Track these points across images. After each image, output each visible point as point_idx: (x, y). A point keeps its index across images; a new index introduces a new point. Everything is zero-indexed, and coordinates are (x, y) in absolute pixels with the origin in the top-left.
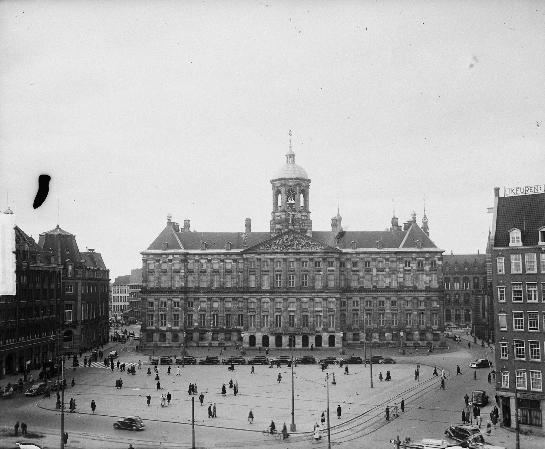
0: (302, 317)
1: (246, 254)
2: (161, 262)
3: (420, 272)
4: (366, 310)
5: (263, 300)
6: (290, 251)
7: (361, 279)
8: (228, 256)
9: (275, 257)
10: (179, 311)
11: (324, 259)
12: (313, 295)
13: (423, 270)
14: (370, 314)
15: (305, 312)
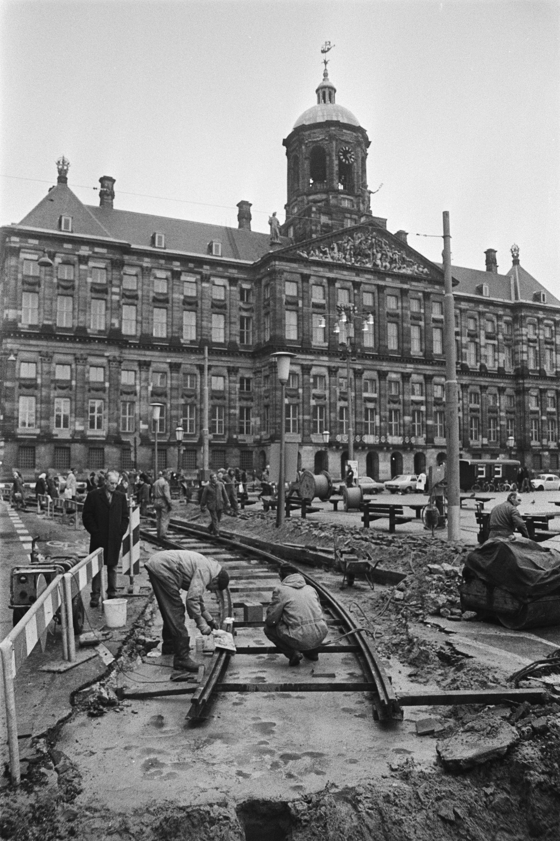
0: (388, 414)
1: (281, 259)
2: (58, 260)
3: (549, 346)
4: (472, 410)
5: (314, 371)
6: (369, 265)
7: (464, 350)
8: (220, 269)
9: (338, 276)
10: (103, 390)
11: (426, 296)
12: (409, 368)
13: (552, 343)
14: (476, 418)
15: (395, 402)
